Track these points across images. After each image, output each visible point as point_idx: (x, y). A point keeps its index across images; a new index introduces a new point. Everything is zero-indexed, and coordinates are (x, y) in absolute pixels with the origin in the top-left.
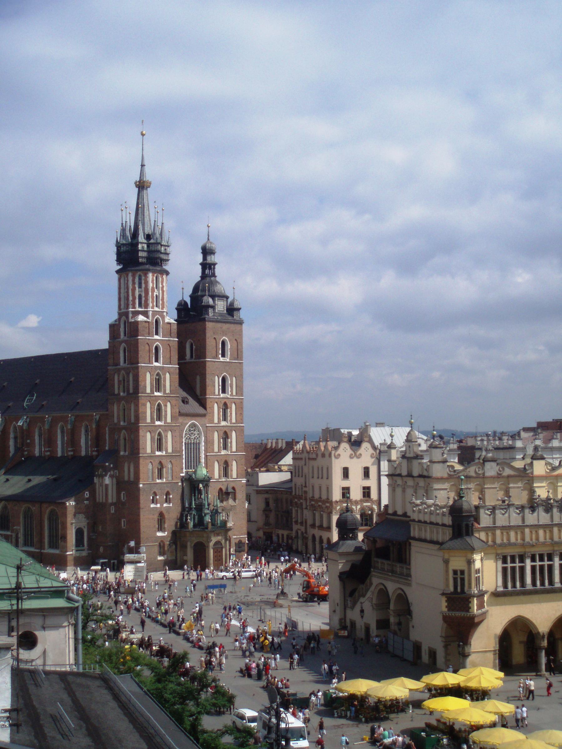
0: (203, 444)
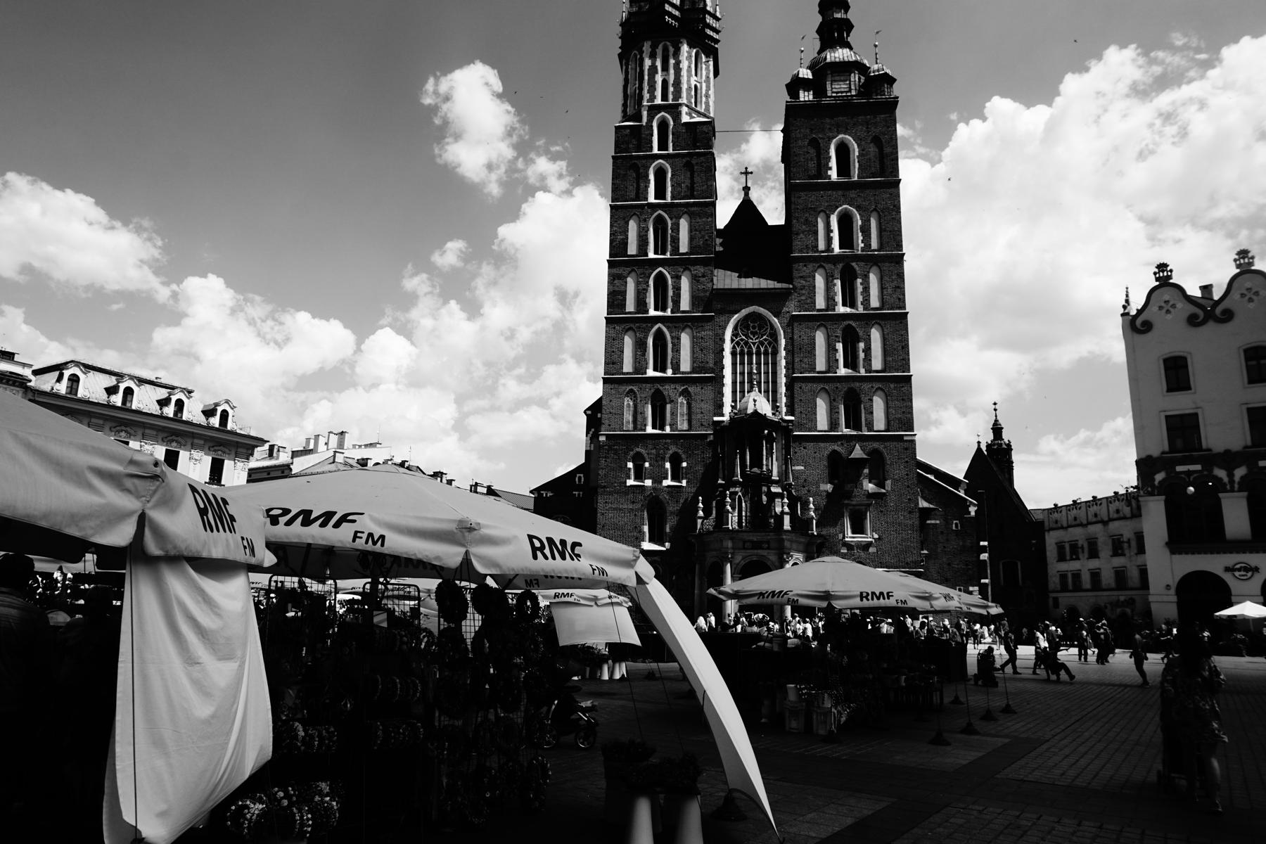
0: (783, 353)
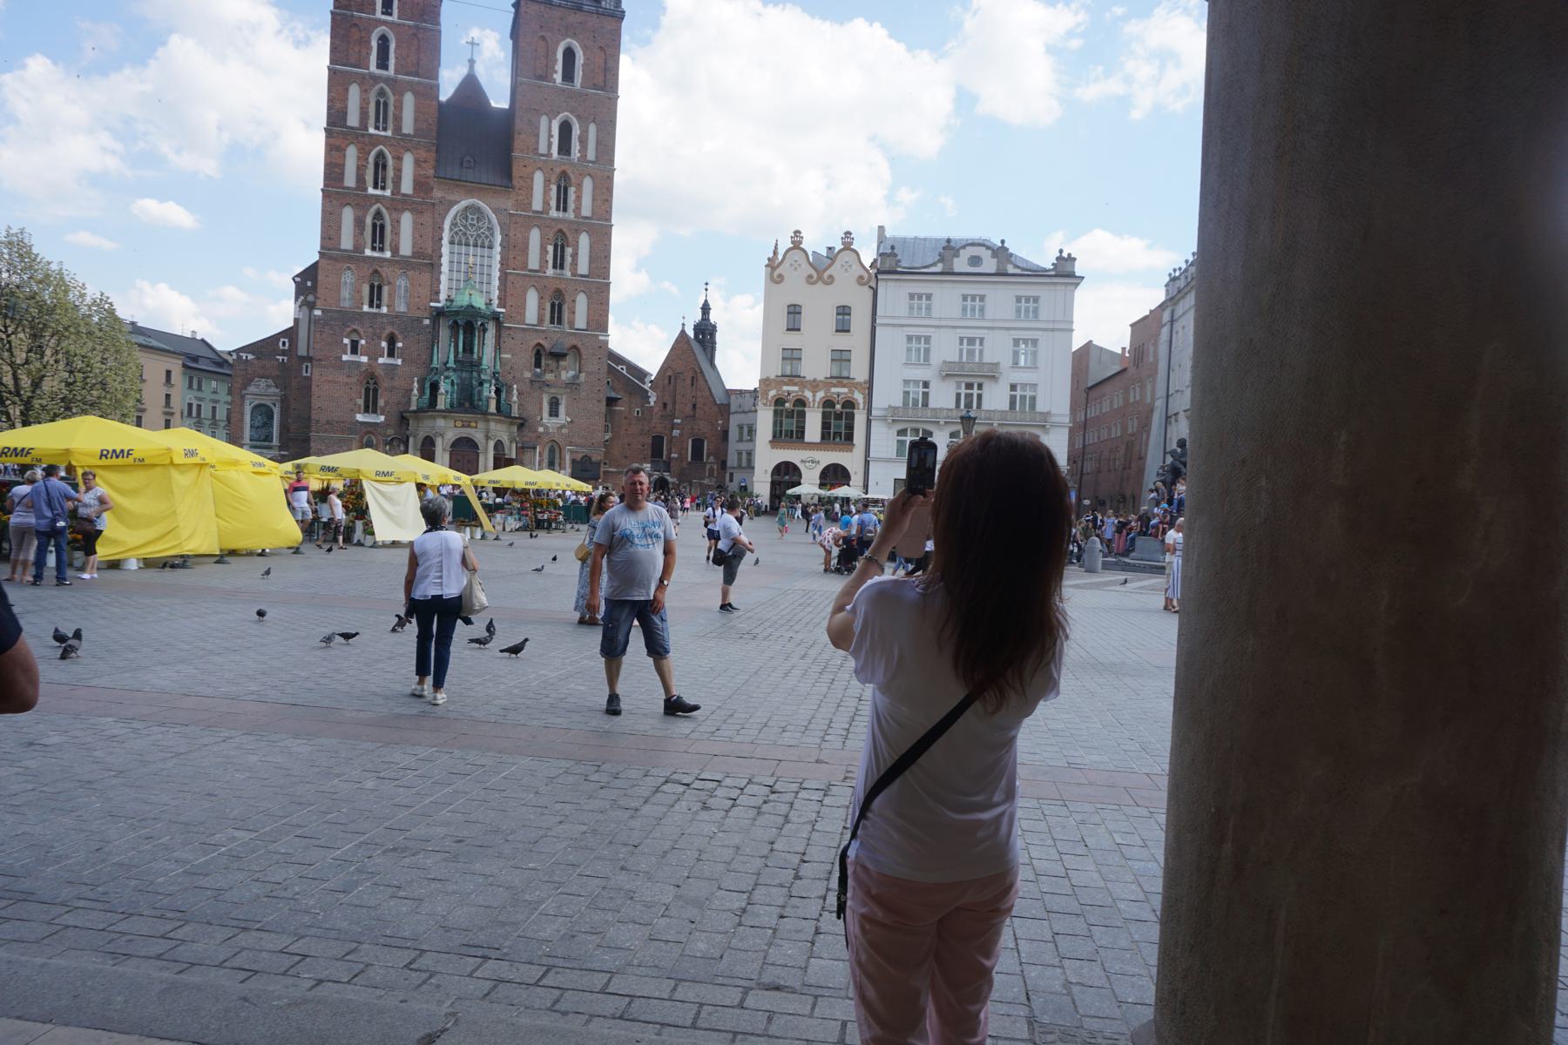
0: (498, 249)
